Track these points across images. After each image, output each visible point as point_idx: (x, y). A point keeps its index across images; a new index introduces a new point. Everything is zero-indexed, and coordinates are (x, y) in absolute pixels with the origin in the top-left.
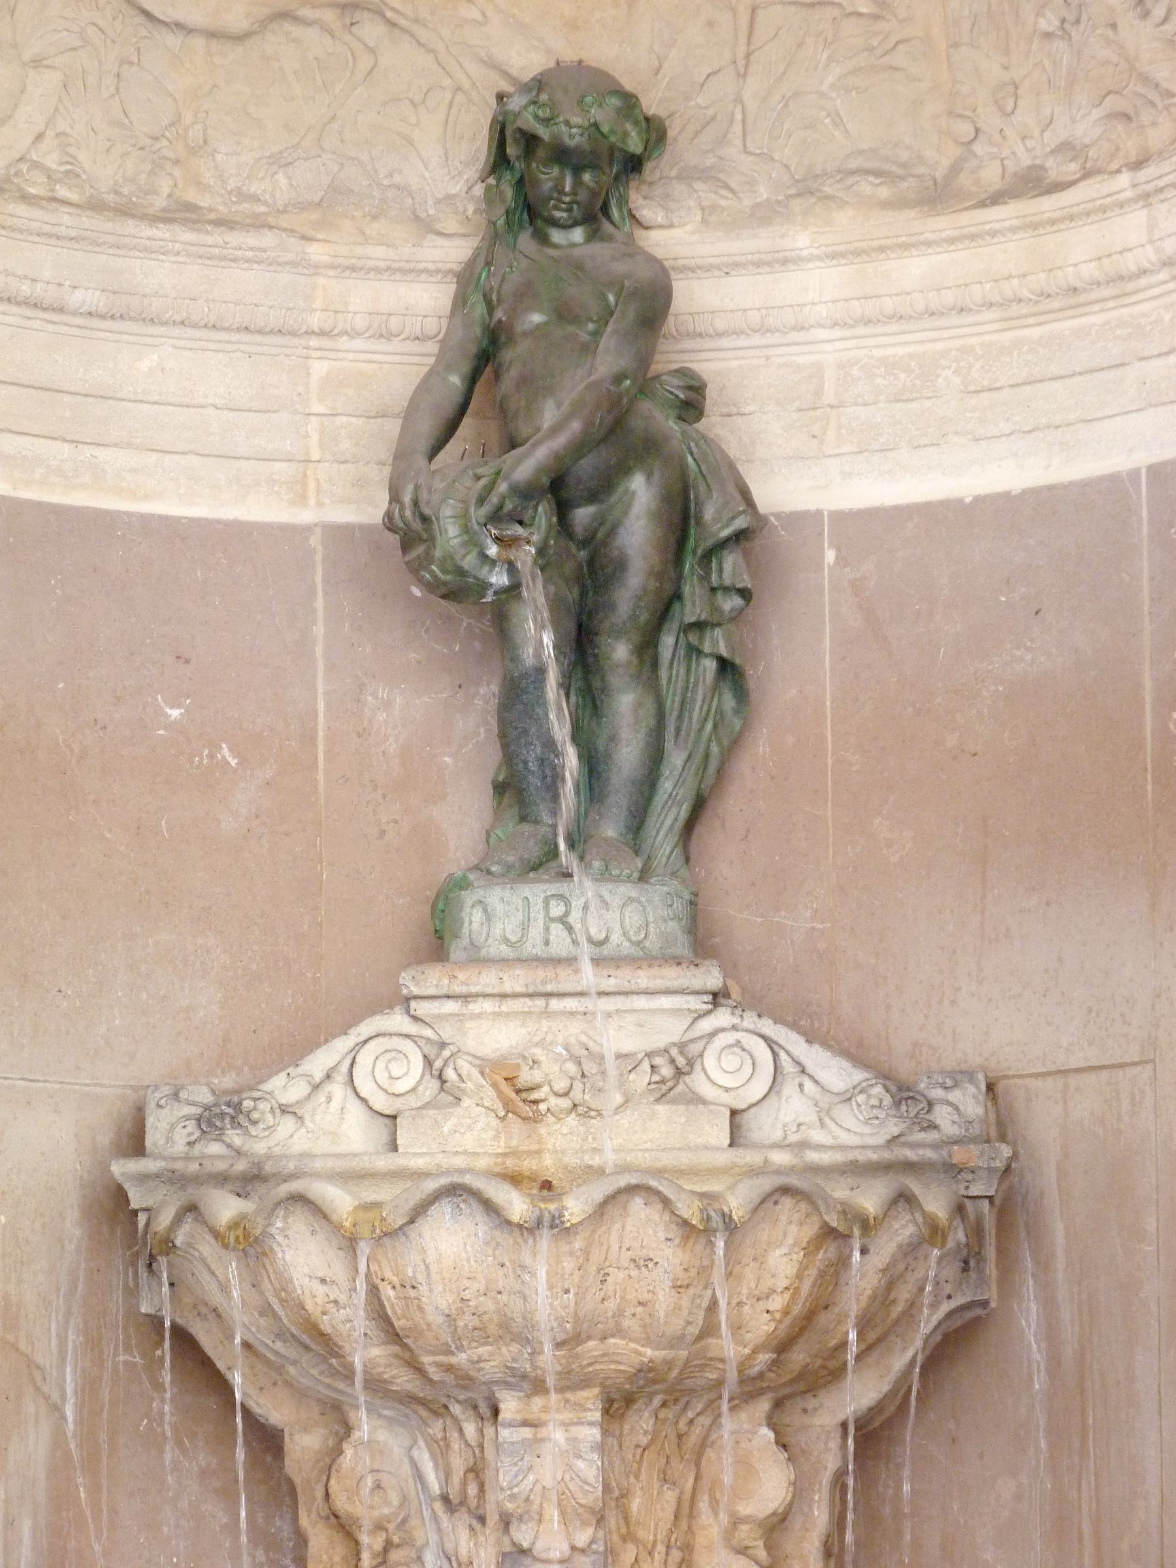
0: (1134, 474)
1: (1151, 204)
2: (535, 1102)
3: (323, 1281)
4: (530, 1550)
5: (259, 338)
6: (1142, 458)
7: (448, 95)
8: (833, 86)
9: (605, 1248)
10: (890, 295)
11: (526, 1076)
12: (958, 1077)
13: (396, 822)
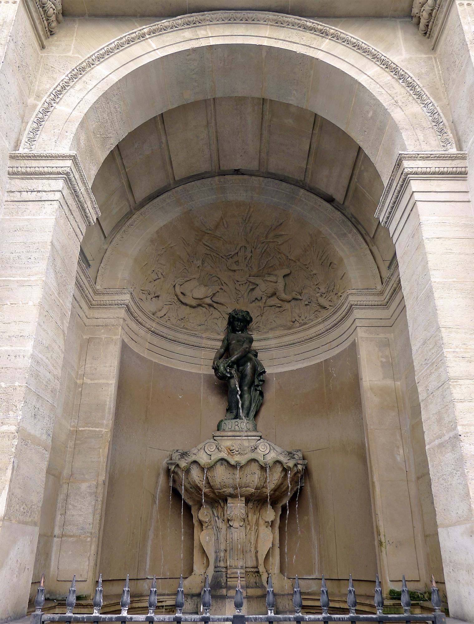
2: (233, 452)
4: (232, 526)
6: (322, 360)
7: (222, 318)
8: (275, 317)
11: (232, 448)
12: (298, 451)
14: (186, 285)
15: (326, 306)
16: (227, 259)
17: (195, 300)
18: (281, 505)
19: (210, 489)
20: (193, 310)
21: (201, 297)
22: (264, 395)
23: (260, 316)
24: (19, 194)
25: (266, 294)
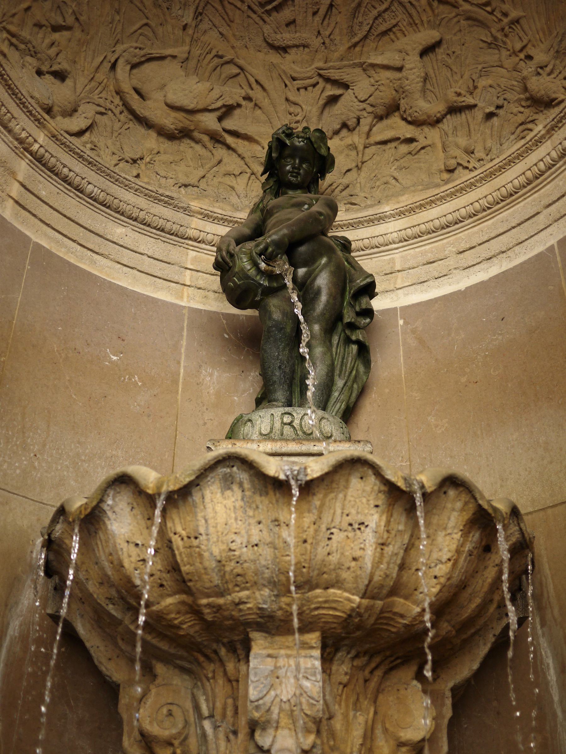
1: (553, 135)
5: (168, 236)
7: (249, 175)
9: (332, 511)
10: (424, 223)
13: (211, 420)
14: (148, 68)
15: (554, 96)
16: (265, 17)
17: (174, 114)
18: (451, 684)
19: (184, 597)
20: (166, 145)
21: (191, 106)
22: (372, 365)
23: (356, 169)
25: (372, 106)
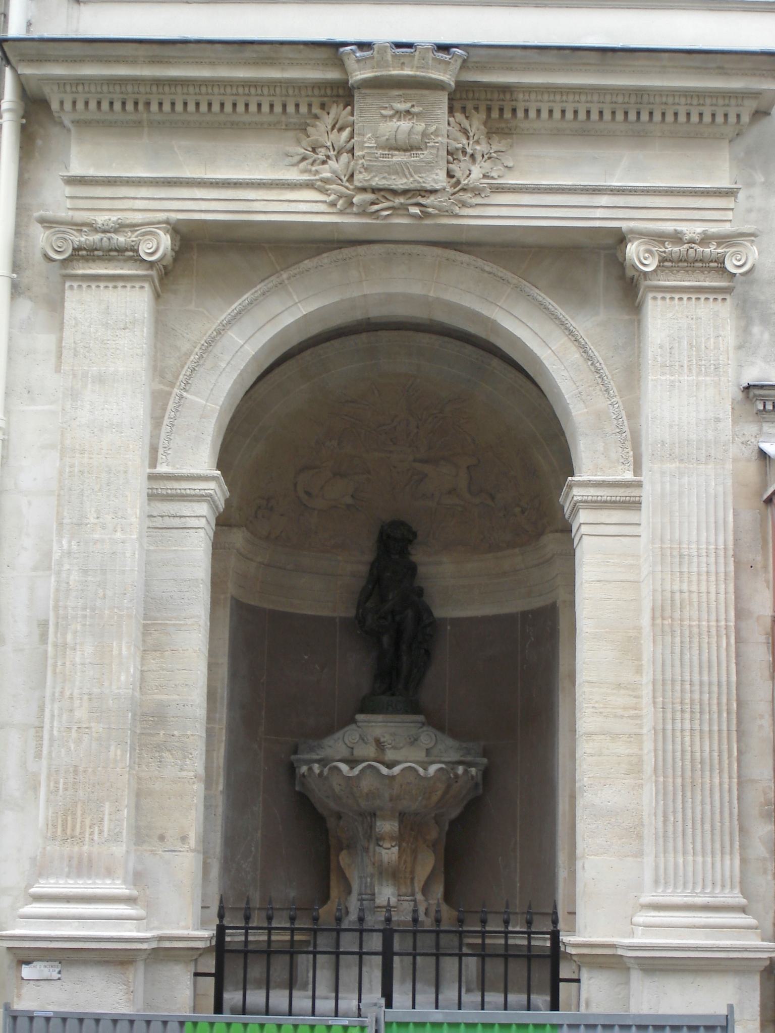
0: (517, 613)
3: (340, 785)
11: (382, 740)
24: (160, 518)
